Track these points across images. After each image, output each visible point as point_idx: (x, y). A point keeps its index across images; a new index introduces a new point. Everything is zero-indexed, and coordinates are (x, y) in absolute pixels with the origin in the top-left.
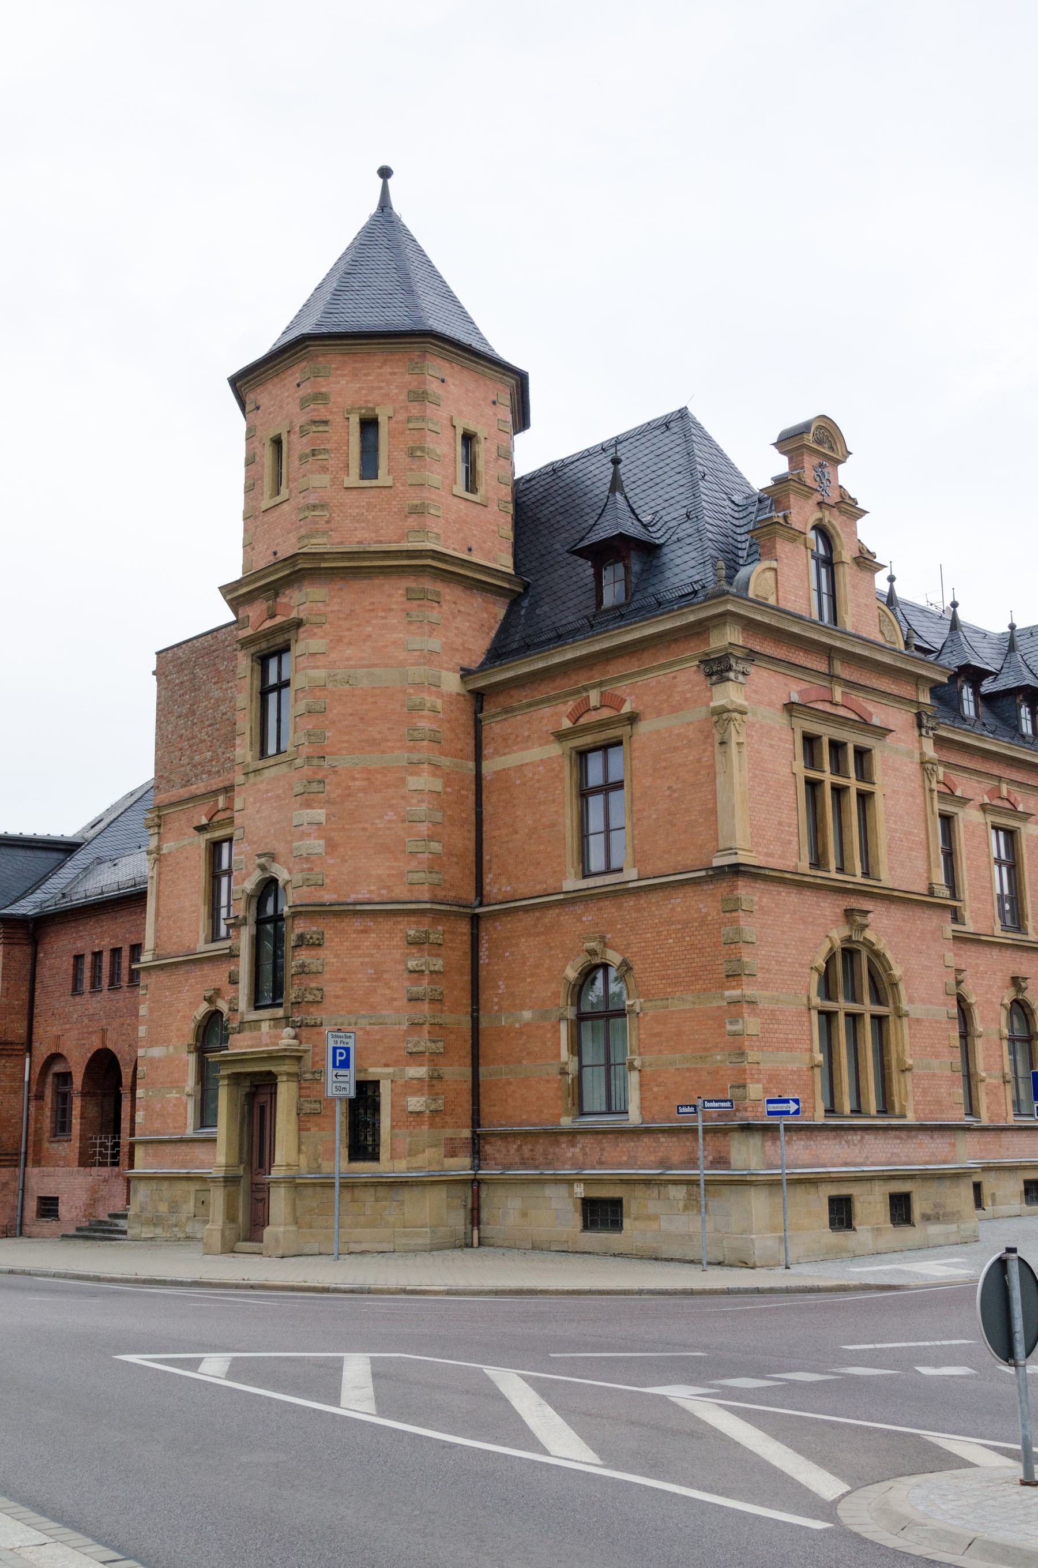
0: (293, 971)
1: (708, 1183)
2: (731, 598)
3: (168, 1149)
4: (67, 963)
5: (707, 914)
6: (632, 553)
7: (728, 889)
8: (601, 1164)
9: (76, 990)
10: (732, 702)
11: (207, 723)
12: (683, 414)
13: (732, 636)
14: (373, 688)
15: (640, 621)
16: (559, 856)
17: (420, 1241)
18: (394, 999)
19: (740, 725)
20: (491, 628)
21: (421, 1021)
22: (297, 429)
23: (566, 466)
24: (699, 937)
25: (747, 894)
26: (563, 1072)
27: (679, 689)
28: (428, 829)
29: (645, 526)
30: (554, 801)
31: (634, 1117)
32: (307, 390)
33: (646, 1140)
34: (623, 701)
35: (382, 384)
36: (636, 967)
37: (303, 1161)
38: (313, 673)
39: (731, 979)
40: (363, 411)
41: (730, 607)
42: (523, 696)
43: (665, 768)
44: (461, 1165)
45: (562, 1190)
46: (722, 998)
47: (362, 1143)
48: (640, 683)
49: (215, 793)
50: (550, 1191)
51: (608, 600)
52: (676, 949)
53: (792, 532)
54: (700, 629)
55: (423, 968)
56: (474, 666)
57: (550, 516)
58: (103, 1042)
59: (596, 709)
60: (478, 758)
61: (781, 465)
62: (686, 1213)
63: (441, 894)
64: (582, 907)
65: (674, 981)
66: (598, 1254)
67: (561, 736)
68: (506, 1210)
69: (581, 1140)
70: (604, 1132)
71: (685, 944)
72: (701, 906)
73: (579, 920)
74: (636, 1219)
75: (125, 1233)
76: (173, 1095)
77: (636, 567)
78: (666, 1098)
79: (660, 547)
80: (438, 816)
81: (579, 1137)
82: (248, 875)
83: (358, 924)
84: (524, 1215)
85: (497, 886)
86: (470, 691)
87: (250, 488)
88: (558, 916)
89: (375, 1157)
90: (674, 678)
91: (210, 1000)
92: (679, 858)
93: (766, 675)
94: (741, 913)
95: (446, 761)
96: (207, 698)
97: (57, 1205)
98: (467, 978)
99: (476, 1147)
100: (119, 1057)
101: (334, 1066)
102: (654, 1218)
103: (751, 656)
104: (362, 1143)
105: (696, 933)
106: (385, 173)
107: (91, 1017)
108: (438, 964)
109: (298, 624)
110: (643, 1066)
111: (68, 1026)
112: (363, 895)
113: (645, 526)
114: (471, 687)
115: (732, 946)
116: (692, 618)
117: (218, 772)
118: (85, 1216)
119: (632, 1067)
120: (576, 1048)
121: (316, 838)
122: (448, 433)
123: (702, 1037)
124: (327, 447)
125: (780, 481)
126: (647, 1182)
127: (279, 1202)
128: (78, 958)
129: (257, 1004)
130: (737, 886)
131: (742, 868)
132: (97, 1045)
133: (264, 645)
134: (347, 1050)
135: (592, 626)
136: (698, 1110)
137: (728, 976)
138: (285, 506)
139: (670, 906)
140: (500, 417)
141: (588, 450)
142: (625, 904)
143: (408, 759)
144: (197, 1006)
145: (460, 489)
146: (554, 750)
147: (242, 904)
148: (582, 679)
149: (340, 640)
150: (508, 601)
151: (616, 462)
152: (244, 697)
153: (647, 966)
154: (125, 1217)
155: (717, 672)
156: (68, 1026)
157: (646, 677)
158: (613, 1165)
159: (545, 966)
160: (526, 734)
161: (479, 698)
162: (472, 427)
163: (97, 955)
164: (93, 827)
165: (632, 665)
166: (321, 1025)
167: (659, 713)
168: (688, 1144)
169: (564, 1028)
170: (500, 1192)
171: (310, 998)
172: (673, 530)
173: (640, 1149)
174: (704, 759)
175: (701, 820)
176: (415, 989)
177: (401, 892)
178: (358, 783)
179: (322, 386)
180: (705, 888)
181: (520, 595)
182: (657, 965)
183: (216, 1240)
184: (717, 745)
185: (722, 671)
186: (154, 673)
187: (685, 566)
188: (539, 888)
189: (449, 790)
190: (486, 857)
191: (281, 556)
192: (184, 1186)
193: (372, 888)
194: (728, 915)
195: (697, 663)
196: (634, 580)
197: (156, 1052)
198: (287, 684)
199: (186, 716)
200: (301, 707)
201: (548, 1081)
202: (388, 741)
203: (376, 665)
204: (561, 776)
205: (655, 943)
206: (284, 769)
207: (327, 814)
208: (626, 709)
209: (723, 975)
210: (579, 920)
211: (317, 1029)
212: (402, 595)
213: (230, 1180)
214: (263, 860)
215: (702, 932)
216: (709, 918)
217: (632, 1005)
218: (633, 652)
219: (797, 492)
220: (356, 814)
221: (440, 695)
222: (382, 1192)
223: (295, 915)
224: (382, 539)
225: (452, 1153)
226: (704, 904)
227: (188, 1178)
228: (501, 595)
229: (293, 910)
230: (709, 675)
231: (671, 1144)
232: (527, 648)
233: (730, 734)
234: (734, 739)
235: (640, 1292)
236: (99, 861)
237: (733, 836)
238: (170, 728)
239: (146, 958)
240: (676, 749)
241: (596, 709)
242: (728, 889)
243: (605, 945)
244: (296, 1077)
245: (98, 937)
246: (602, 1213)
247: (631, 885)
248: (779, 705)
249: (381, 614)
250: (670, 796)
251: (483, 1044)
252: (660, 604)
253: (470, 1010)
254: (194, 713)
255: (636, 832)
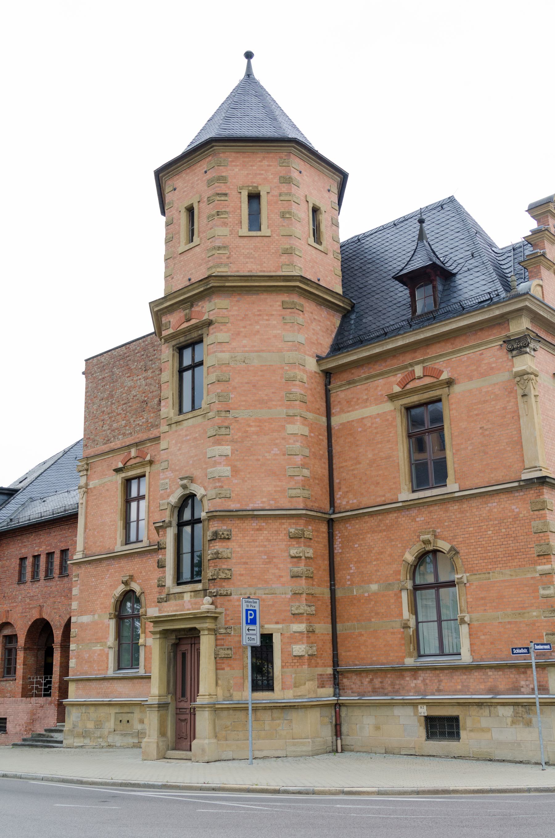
0: (209, 557)
1: (542, 704)
2: (529, 297)
3: (94, 684)
4: (15, 563)
5: (518, 513)
6: (438, 278)
7: (536, 495)
8: (439, 691)
9: (21, 581)
10: (530, 367)
11: (122, 402)
12: (451, 200)
13: (521, 325)
14: (261, 366)
15: (457, 316)
16: (394, 478)
17: (305, 749)
18: (281, 577)
19: (535, 384)
20: (332, 332)
21: (300, 592)
22: (205, 199)
23: (367, 236)
24: (514, 529)
25: (549, 498)
26: (406, 627)
27: (486, 361)
28: (301, 460)
29: (442, 262)
30: (389, 441)
31: (466, 658)
32: (212, 174)
33: (476, 674)
34: (441, 372)
35: (262, 172)
36: (461, 552)
37: (220, 691)
38: (220, 355)
39: (541, 558)
40: (250, 188)
41: (527, 303)
42: (363, 373)
43: (477, 415)
44: (327, 694)
45: (409, 711)
46: (535, 571)
47: (262, 679)
48: (453, 360)
49: (129, 446)
50: (398, 711)
51: (419, 311)
52: (494, 538)
53: (549, 263)
54: (502, 320)
55: (301, 555)
56: (324, 355)
57: (362, 265)
58: (41, 614)
59: (419, 378)
60: (329, 415)
61: (533, 224)
62: (514, 726)
63: (310, 504)
64: (416, 511)
65: (495, 560)
66: (440, 757)
67: (392, 397)
68: (362, 725)
69: (422, 675)
70: (442, 669)
71: (501, 534)
72: (514, 507)
73: (414, 520)
74: (471, 731)
75: (61, 742)
76: (98, 648)
77: (440, 288)
78: (492, 643)
79: (454, 275)
80: (307, 452)
81: (420, 672)
82: (173, 492)
83: (255, 524)
84: (377, 728)
85: (346, 500)
86: (321, 371)
87: (168, 241)
88: (397, 518)
89: (270, 687)
90: (482, 354)
91: (126, 583)
92: (492, 476)
93: (543, 353)
94: (547, 512)
95: (310, 416)
96: (122, 386)
97: (6, 723)
98: (327, 562)
99: (336, 679)
100: (52, 623)
101: (247, 623)
102: (487, 730)
103: (538, 339)
104: (262, 679)
105: (511, 526)
106: (249, 55)
107: (31, 598)
108: (310, 553)
109: (209, 323)
110: (470, 621)
111: (15, 604)
112: (258, 505)
113: (442, 262)
114: (324, 368)
115: (541, 535)
116: (497, 313)
117: (131, 433)
118: (26, 731)
119: (463, 621)
120: (414, 610)
121: (224, 465)
122: (304, 205)
123: (519, 599)
124: (227, 210)
125: (534, 232)
126: (480, 704)
127: (203, 722)
128: (23, 560)
129: (179, 582)
130: (543, 492)
131: (548, 480)
132: (35, 616)
133: (182, 339)
134: (255, 611)
135: (411, 326)
136: (531, 651)
137: (539, 556)
138: (197, 249)
139: (487, 508)
140: (332, 199)
141: (383, 226)
142: (451, 508)
143: (286, 413)
144: (116, 588)
145: (311, 240)
146: (389, 406)
147: (168, 512)
148: (408, 359)
149: (238, 334)
150: (341, 315)
151: (421, 221)
152: (168, 375)
153: (470, 550)
154: (61, 731)
155: (517, 348)
156: (15, 604)
157: (459, 355)
158: (447, 693)
159: (388, 553)
160: (365, 397)
161: (328, 375)
162: (318, 204)
163: (36, 557)
164: (20, 482)
165: (449, 348)
166: (231, 595)
167: (470, 379)
168: (512, 676)
169: (405, 596)
170: (357, 712)
171: (223, 576)
172: (462, 264)
173: (472, 680)
174: (508, 408)
175: (509, 449)
176: (295, 569)
177: (284, 503)
178: (253, 429)
179: (223, 172)
180: (517, 494)
181: (349, 312)
182: (479, 549)
183: (153, 750)
184: (519, 397)
185: (521, 347)
186: (83, 373)
187: (473, 285)
188: (379, 500)
189: (312, 435)
190: (336, 481)
191: (193, 281)
192: (107, 710)
193: (264, 500)
194: (536, 513)
195: (502, 343)
196: (439, 295)
197: (85, 619)
198: (201, 364)
199: (107, 398)
200: (213, 378)
201: (393, 633)
202: (272, 401)
203: (263, 351)
204: (394, 424)
205: (476, 534)
206: (199, 420)
207: (232, 450)
208: (444, 376)
209: (535, 555)
210: (414, 520)
211: (228, 598)
212: (279, 306)
213: (162, 706)
214: (185, 482)
215: (515, 526)
216: (521, 515)
217: (461, 578)
218: (447, 339)
219: (548, 239)
220: (252, 449)
221: (305, 371)
222: (276, 713)
223: (210, 518)
224: (265, 269)
225: (322, 686)
226: (518, 506)
227: (110, 705)
228: (337, 311)
229: (210, 514)
230: (511, 351)
231: (497, 677)
232: (361, 342)
233: (530, 389)
234: (533, 393)
235: (529, 790)
236: (32, 500)
237: (537, 459)
238: (95, 407)
239: (78, 556)
240: (485, 402)
241: (419, 378)
242: (536, 495)
243: (436, 536)
244: (214, 631)
245: (39, 545)
246: (442, 727)
247: (457, 495)
248: (551, 374)
249: (267, 318)
250: (482, 434)
251: (339, 607)
252: (464, 309)
253: (329, 584)
254: (112, 396)
255: (456, 459)
